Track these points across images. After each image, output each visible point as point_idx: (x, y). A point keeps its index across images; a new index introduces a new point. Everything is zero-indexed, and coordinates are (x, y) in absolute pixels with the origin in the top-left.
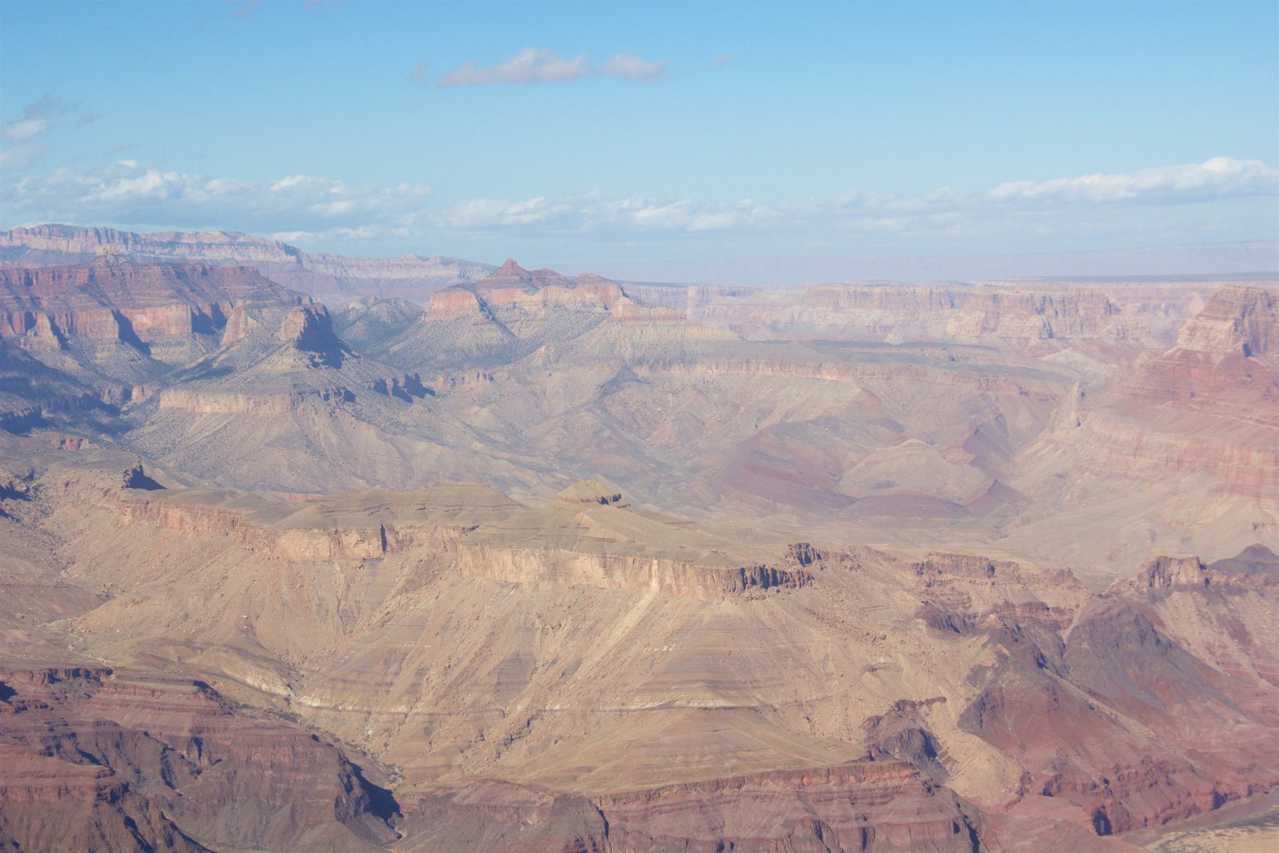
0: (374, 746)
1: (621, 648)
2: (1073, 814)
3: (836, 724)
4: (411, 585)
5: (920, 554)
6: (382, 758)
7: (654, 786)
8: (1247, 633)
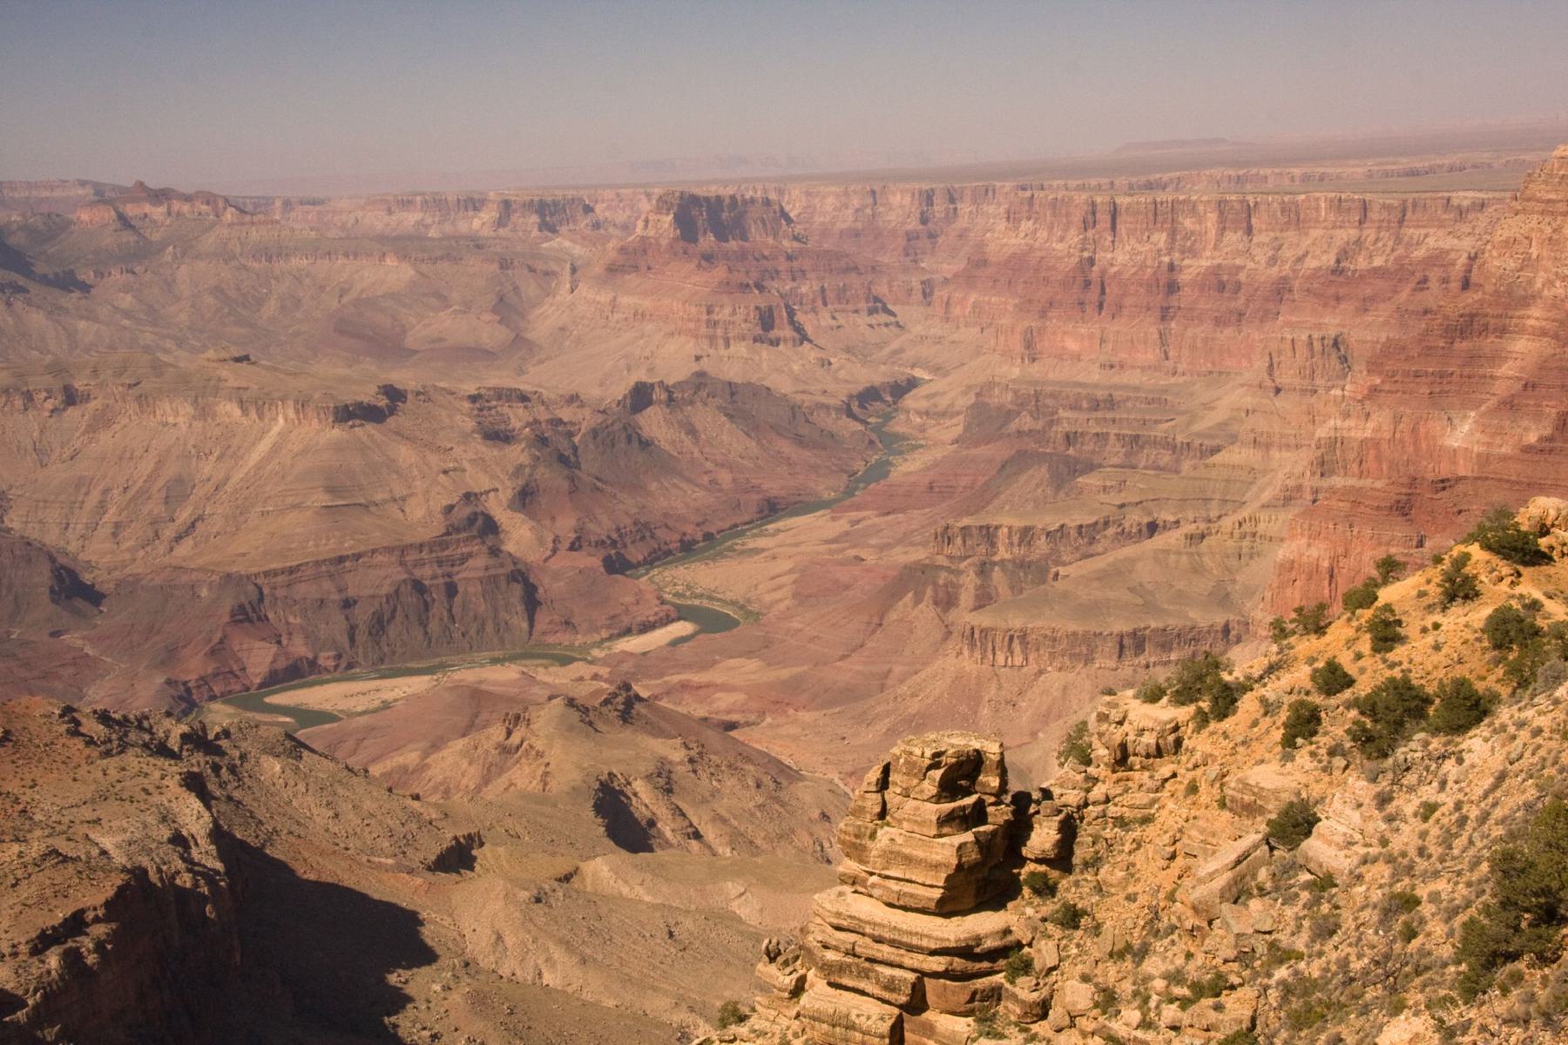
0: (73, 547)
1: (259, 467)
2: (591, 561)
3: (423, 513)
4: (92, 429)
5: (471, 388)
6: (81, 557)
7: (295, 563)
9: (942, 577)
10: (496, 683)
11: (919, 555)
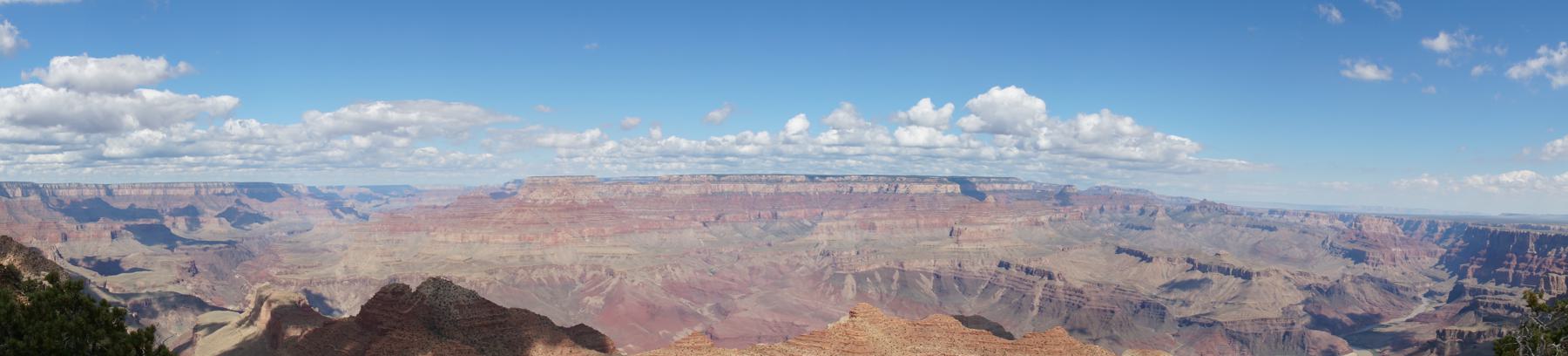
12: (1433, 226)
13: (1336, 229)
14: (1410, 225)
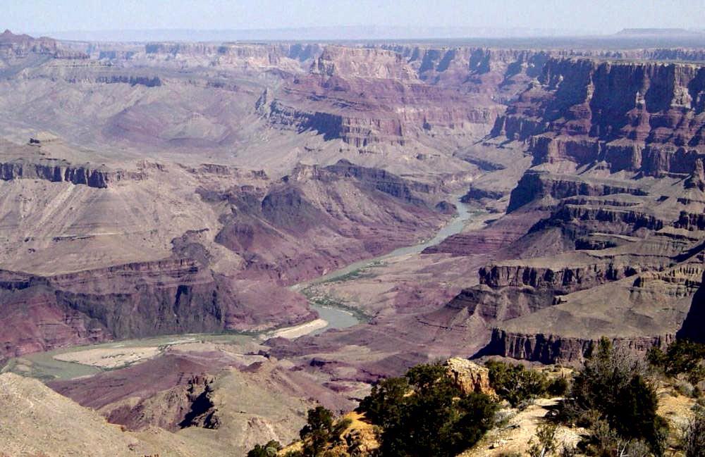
8: (340, 198)
9: (487, 299)
10: (197, 354)
11: (474, 282)
12: (480, 59)
13: (283, 75)
14: (433, 59)
